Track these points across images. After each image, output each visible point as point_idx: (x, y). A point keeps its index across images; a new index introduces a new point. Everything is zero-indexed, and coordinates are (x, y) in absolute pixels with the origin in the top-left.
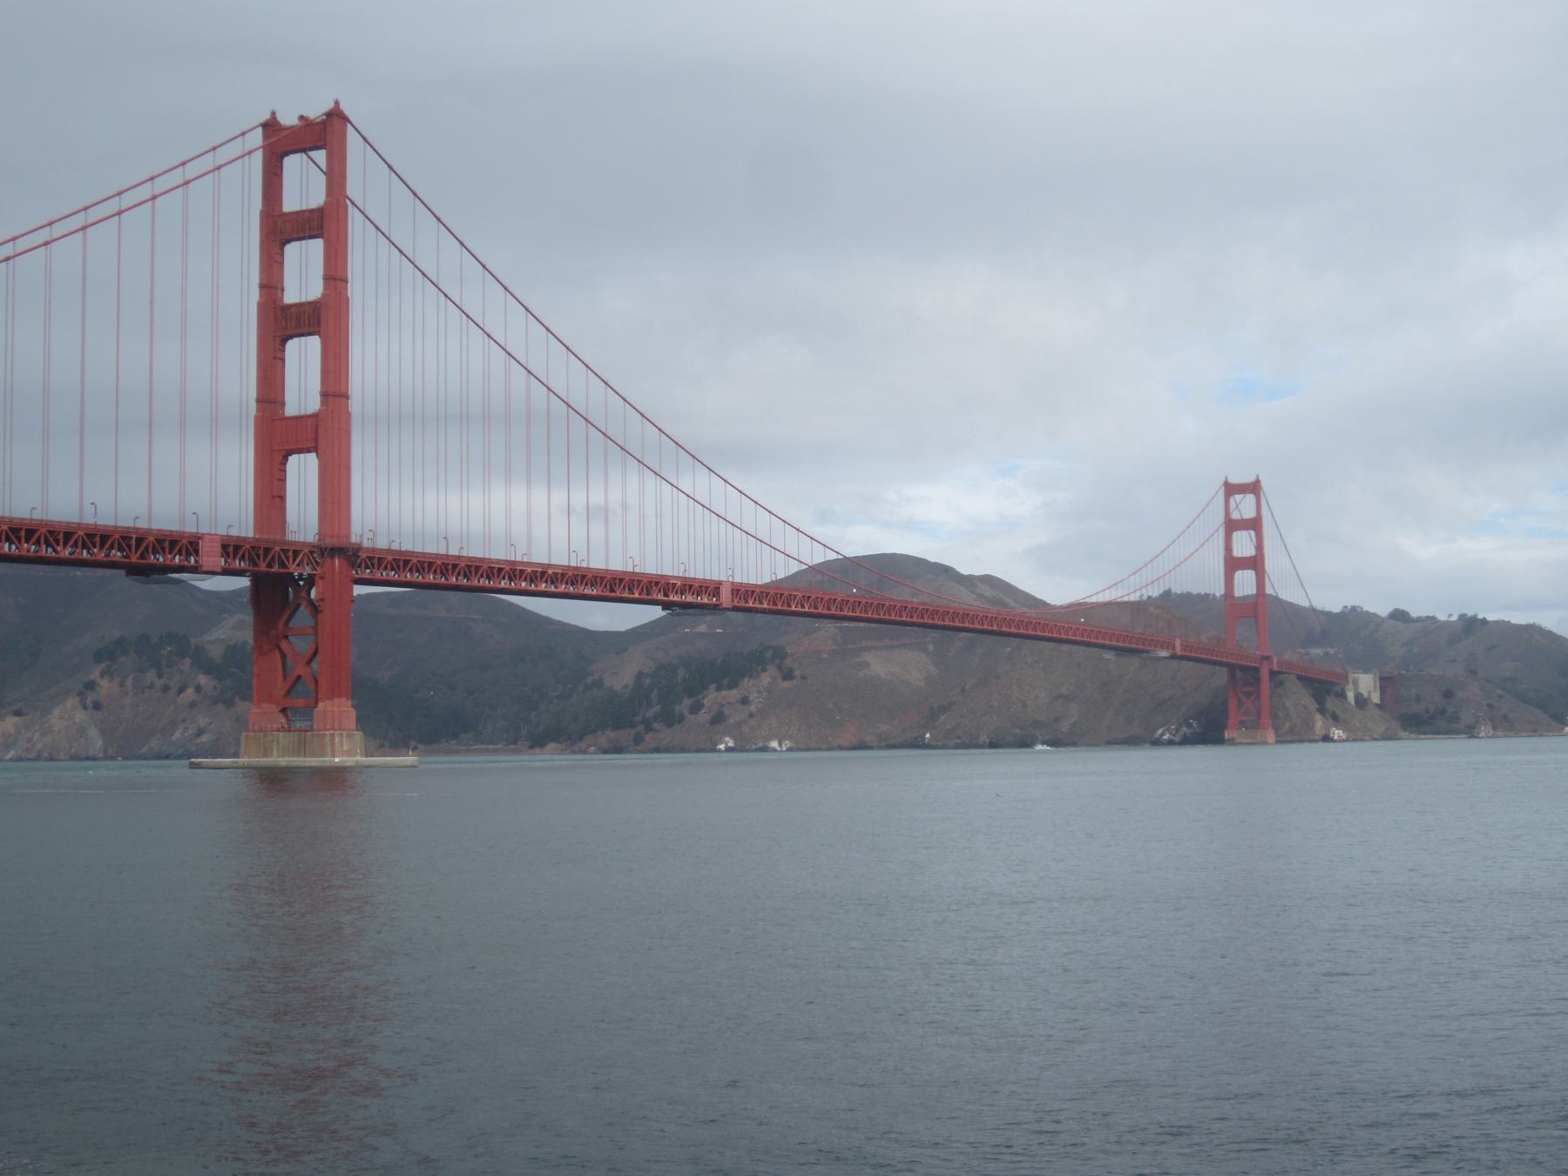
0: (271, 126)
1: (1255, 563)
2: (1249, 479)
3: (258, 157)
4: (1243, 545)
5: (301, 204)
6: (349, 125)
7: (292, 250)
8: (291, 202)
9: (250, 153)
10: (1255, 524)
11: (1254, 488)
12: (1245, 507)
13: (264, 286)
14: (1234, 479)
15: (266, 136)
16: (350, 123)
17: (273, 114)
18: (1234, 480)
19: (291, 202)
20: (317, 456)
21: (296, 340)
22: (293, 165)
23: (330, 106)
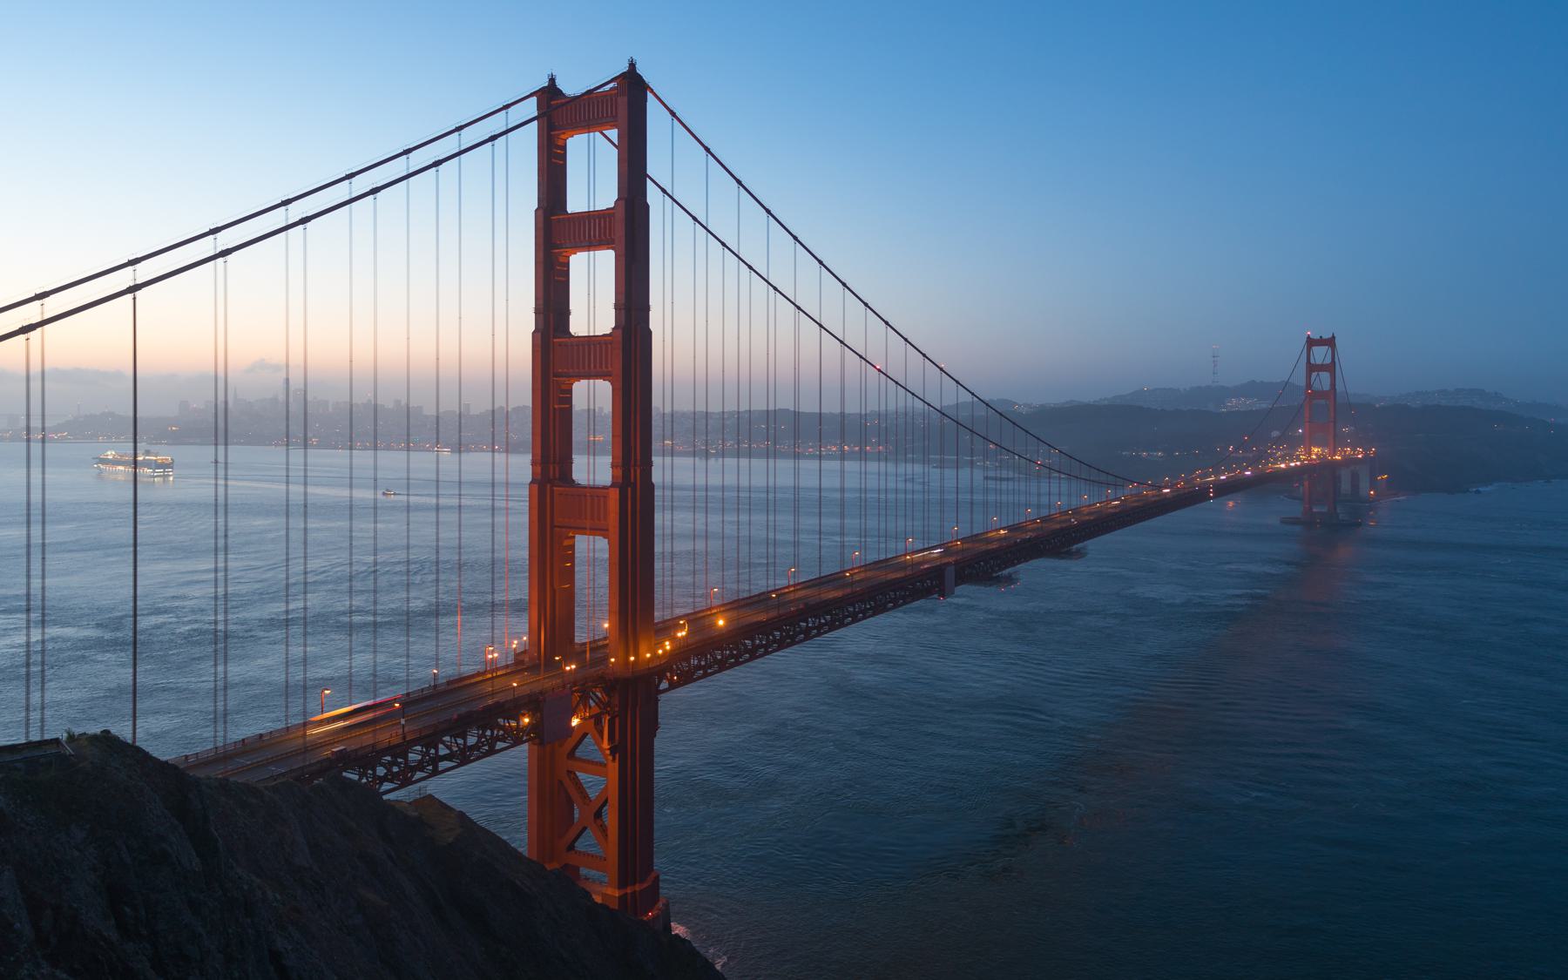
0: (549, 95)
2: (1324, 337)
3: (527, 143)
5: (589, 207)
7: (579, 263)
8: (576, 202)
10: (1331, 368)
11: (1330, 342)
12: (1320, 354)
16: (652, 91)
17: (552, 80)
19: (576, 202)
21: (584, 382)
22: (578, 147)
23: (624, 68)
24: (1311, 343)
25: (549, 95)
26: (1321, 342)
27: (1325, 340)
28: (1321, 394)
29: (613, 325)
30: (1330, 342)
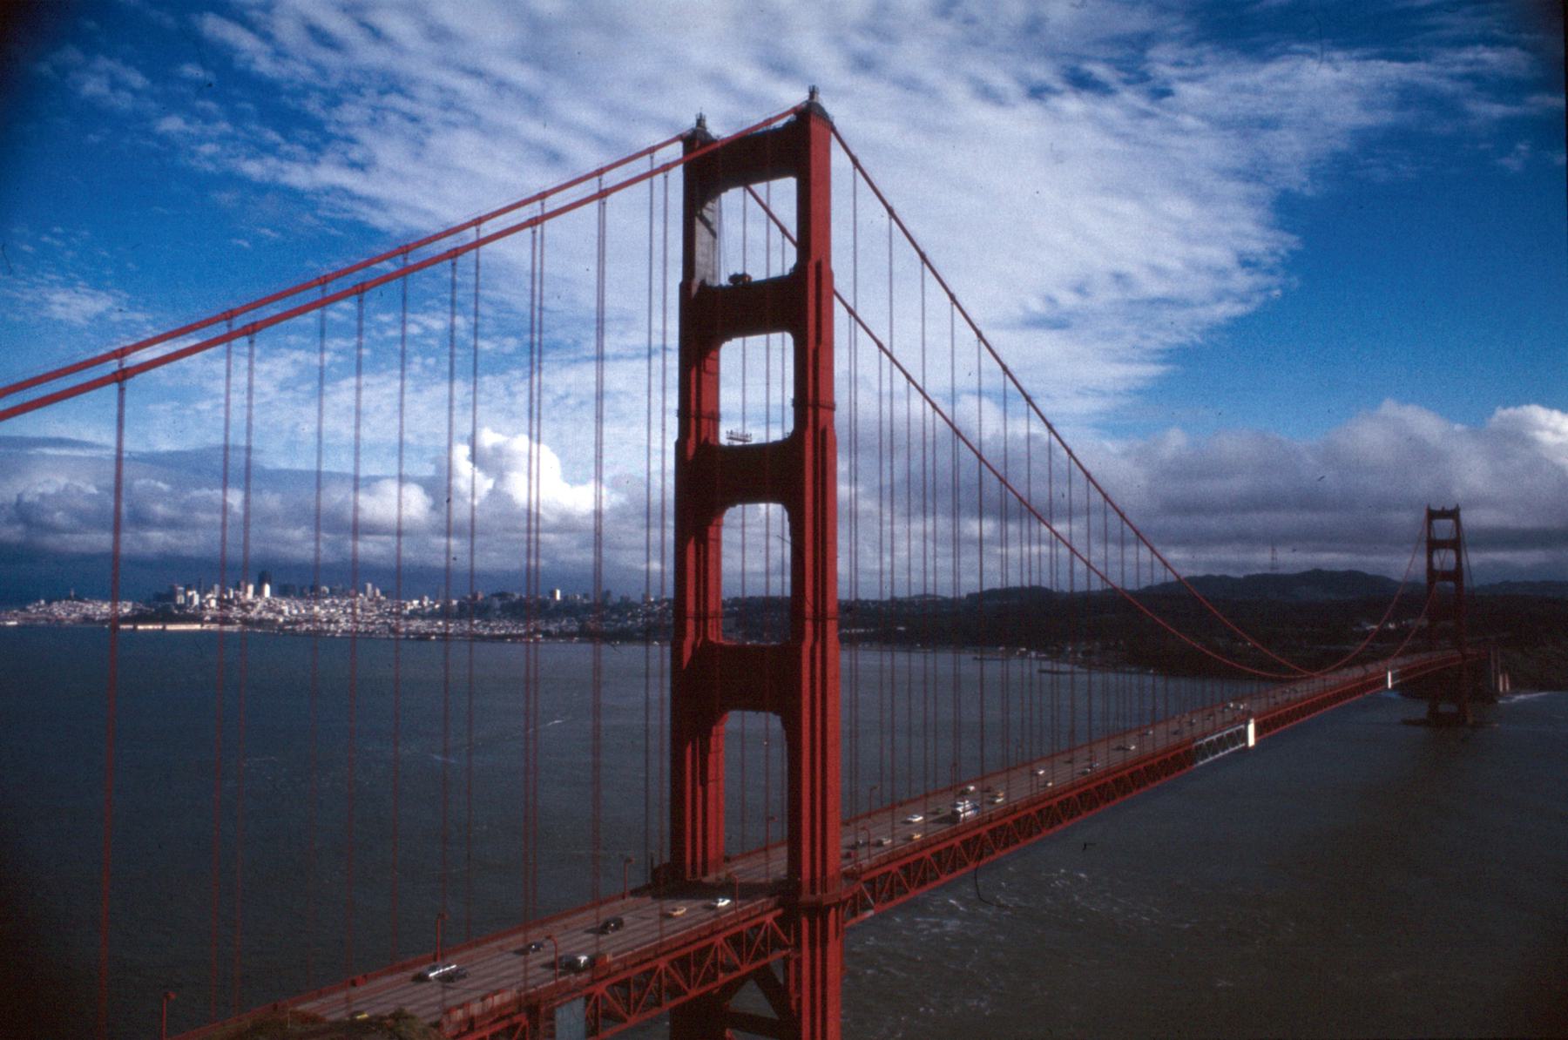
0: (695, 140)
1: (1457, 574)
2: (1450, 507)
4: (1445, 559)
6: (833, 135)
9: (666, 168)
11: (1454, 514)
12: (1444, 528)
13: (684, 413)
14: (1439, 508)
15: (686, 151)
16: (833, 129)
17: (700, 121)
18: (1433, 508)
20: (785, 723)
21: (739, 507)
24: (1432, 515)
25: (695, 140)
26: (1444, 514)
27: (1448, 512)
28: (1446, 575)
29: (790, 427)
30: (1454, 514)
